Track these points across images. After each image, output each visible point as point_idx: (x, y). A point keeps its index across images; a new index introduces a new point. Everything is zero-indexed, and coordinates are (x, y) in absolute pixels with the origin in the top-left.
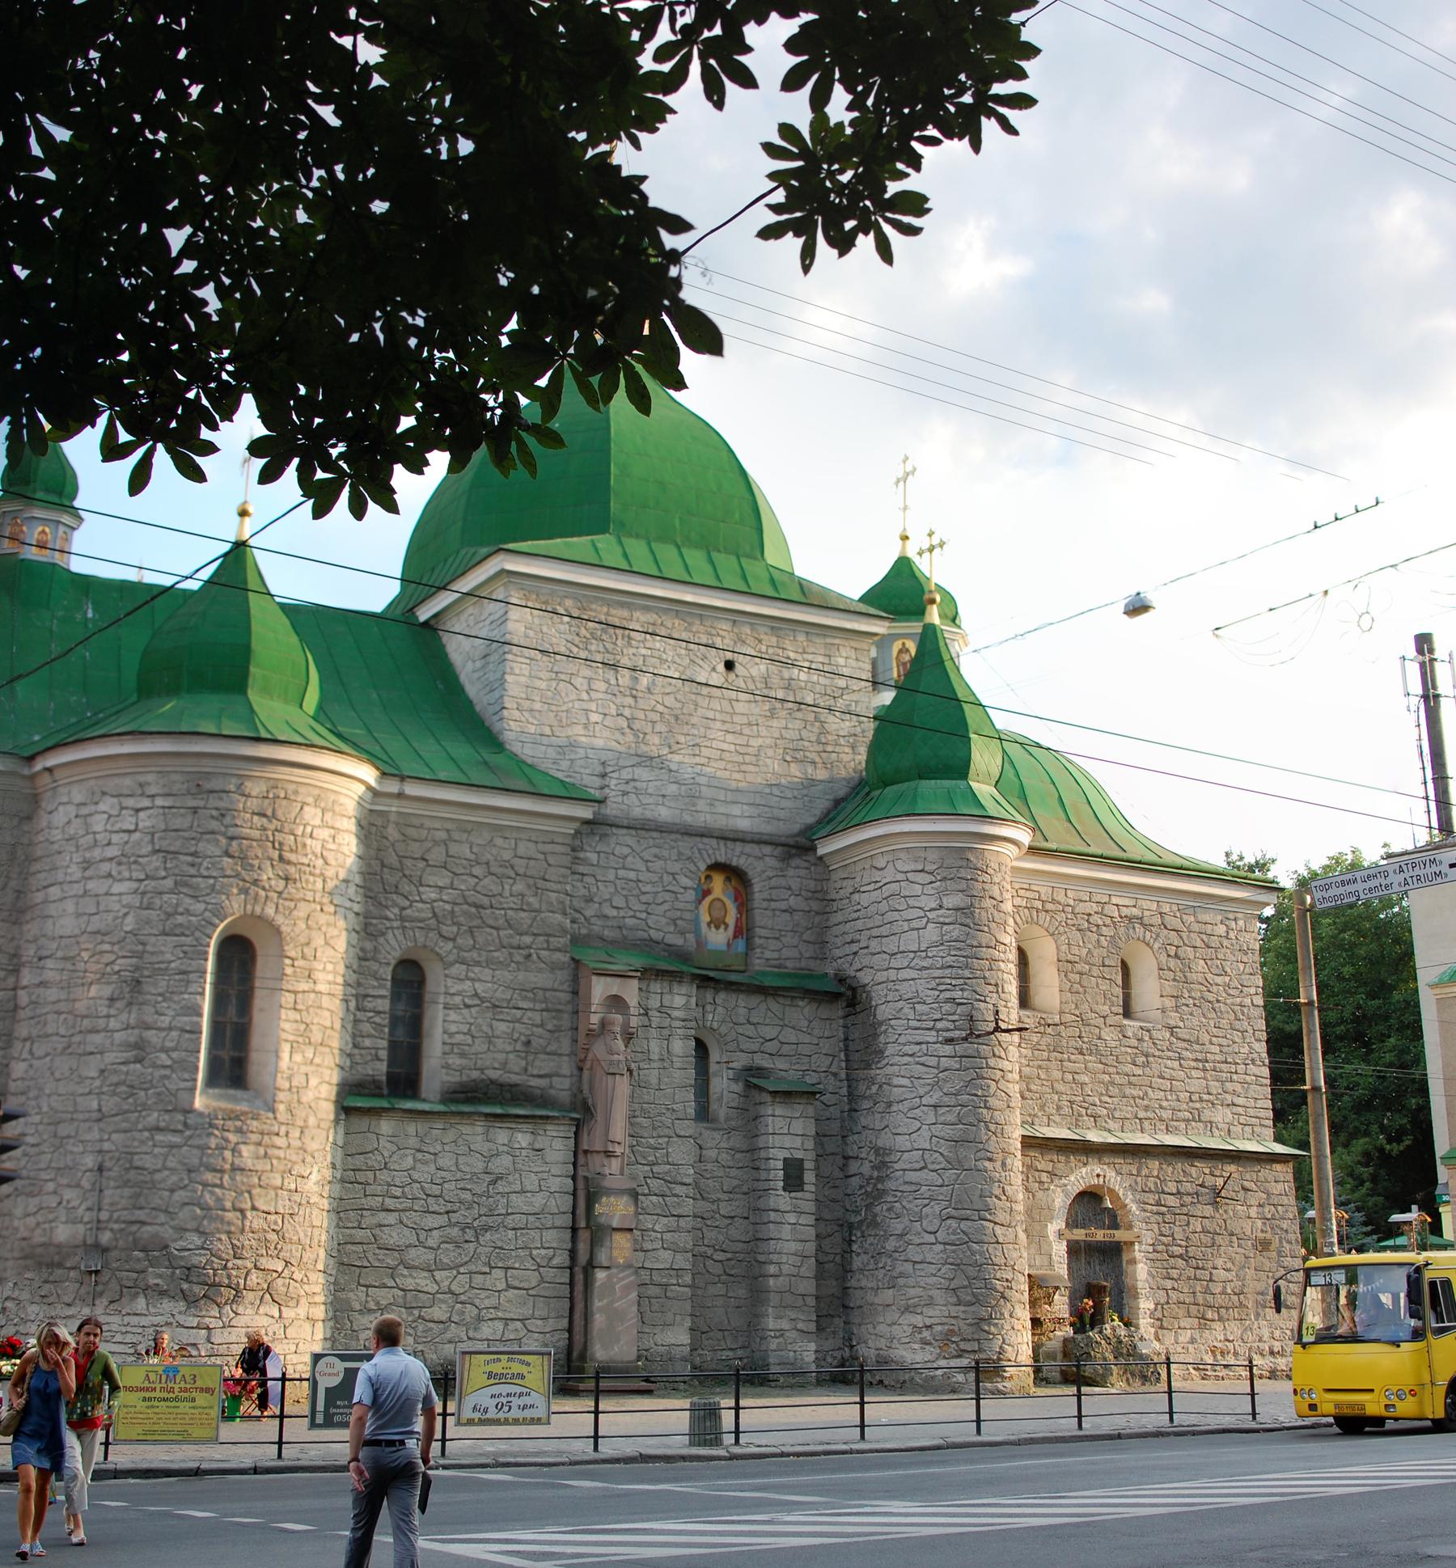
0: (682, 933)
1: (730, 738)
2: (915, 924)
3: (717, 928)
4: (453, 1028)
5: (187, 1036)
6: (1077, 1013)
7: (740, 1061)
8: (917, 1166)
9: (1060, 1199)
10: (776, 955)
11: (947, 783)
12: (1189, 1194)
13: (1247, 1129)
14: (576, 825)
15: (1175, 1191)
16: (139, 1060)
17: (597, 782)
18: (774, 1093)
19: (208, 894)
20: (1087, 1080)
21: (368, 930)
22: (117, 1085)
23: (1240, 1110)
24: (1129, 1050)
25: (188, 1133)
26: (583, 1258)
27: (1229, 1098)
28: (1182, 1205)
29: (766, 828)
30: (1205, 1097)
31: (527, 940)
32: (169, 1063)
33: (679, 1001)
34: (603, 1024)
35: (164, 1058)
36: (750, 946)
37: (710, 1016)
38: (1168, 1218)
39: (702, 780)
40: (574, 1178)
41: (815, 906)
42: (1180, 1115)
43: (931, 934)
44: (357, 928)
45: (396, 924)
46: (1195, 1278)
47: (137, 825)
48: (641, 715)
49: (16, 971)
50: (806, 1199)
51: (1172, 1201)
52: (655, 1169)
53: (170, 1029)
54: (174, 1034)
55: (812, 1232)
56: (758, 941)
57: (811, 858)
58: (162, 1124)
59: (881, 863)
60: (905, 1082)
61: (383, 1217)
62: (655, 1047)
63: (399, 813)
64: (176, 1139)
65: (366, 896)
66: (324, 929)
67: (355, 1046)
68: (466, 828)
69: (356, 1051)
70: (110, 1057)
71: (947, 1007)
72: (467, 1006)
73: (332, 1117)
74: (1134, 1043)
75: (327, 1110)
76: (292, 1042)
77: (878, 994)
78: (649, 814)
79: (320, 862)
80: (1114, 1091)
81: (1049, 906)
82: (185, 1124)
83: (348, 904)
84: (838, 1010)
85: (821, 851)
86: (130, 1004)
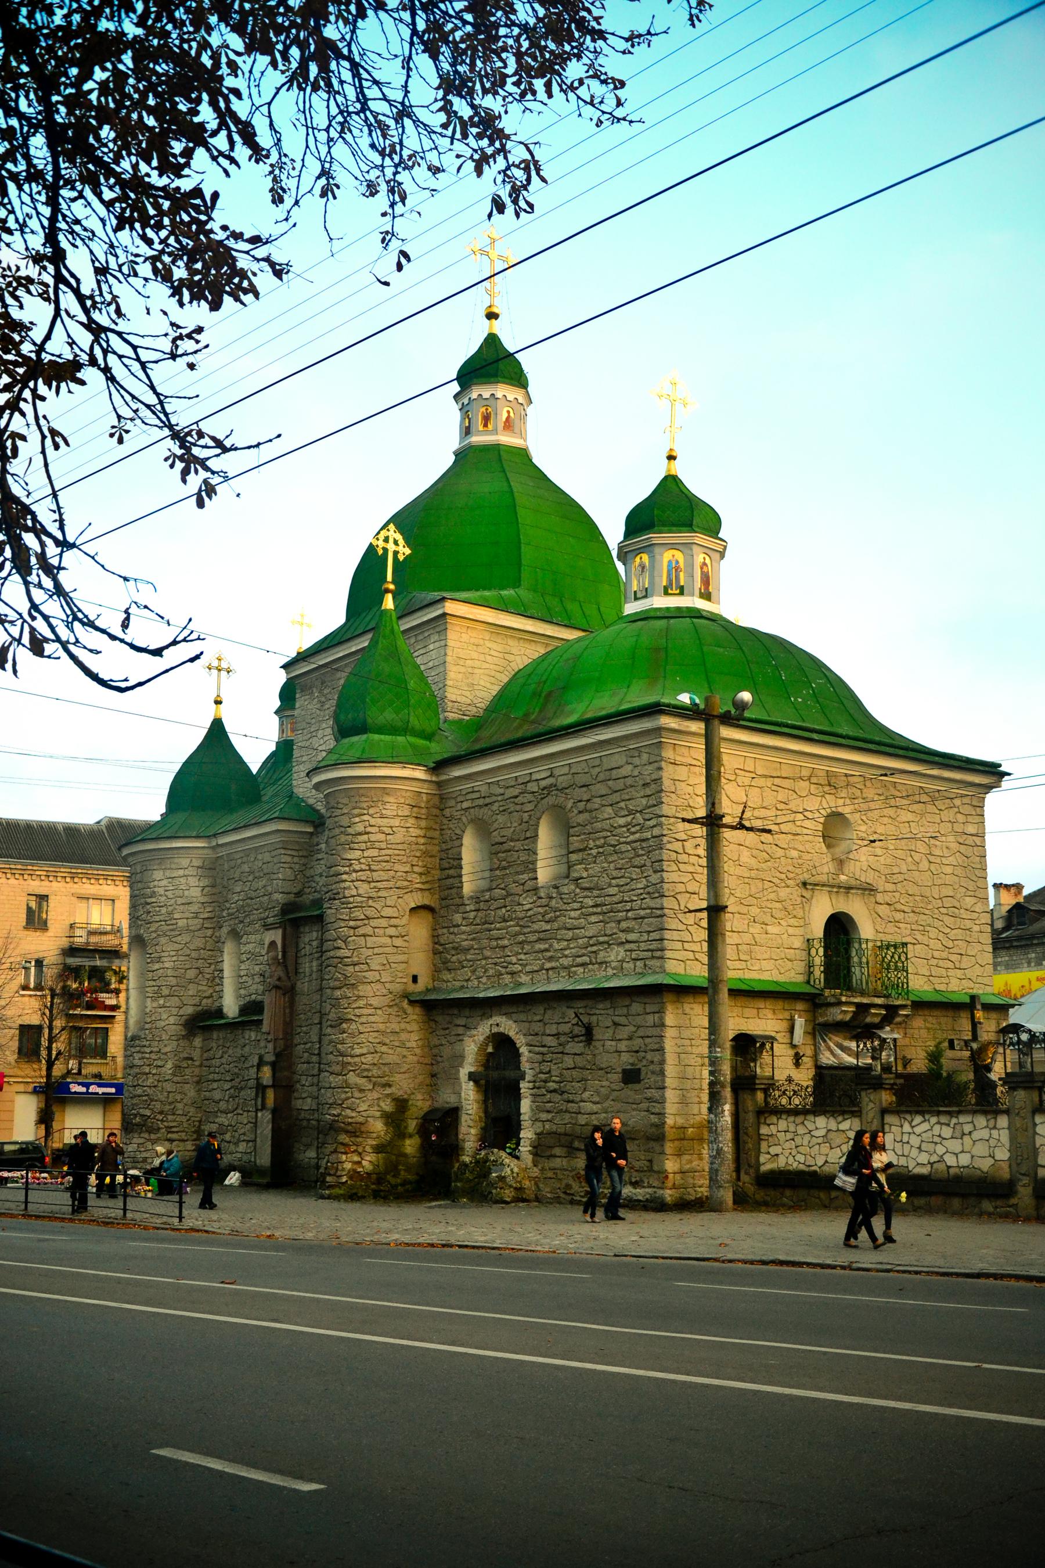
6: (502, 886)
12: (565, 1034)
13: (638, 963)
15: (554, 1032)
20: (506, 942)
23: (633, 946)
24: (541, 910)
27: (623, 937)
28: (560, 1045)
30: (601, 939)
38: (548, 1057)
42: (579, 960)
46: (566, 1111)
51: (550, 1041)
68: (247, 853)
74: (544, 901)
75: (174, 1030)
80: (527, 947)
81: (488, 800)
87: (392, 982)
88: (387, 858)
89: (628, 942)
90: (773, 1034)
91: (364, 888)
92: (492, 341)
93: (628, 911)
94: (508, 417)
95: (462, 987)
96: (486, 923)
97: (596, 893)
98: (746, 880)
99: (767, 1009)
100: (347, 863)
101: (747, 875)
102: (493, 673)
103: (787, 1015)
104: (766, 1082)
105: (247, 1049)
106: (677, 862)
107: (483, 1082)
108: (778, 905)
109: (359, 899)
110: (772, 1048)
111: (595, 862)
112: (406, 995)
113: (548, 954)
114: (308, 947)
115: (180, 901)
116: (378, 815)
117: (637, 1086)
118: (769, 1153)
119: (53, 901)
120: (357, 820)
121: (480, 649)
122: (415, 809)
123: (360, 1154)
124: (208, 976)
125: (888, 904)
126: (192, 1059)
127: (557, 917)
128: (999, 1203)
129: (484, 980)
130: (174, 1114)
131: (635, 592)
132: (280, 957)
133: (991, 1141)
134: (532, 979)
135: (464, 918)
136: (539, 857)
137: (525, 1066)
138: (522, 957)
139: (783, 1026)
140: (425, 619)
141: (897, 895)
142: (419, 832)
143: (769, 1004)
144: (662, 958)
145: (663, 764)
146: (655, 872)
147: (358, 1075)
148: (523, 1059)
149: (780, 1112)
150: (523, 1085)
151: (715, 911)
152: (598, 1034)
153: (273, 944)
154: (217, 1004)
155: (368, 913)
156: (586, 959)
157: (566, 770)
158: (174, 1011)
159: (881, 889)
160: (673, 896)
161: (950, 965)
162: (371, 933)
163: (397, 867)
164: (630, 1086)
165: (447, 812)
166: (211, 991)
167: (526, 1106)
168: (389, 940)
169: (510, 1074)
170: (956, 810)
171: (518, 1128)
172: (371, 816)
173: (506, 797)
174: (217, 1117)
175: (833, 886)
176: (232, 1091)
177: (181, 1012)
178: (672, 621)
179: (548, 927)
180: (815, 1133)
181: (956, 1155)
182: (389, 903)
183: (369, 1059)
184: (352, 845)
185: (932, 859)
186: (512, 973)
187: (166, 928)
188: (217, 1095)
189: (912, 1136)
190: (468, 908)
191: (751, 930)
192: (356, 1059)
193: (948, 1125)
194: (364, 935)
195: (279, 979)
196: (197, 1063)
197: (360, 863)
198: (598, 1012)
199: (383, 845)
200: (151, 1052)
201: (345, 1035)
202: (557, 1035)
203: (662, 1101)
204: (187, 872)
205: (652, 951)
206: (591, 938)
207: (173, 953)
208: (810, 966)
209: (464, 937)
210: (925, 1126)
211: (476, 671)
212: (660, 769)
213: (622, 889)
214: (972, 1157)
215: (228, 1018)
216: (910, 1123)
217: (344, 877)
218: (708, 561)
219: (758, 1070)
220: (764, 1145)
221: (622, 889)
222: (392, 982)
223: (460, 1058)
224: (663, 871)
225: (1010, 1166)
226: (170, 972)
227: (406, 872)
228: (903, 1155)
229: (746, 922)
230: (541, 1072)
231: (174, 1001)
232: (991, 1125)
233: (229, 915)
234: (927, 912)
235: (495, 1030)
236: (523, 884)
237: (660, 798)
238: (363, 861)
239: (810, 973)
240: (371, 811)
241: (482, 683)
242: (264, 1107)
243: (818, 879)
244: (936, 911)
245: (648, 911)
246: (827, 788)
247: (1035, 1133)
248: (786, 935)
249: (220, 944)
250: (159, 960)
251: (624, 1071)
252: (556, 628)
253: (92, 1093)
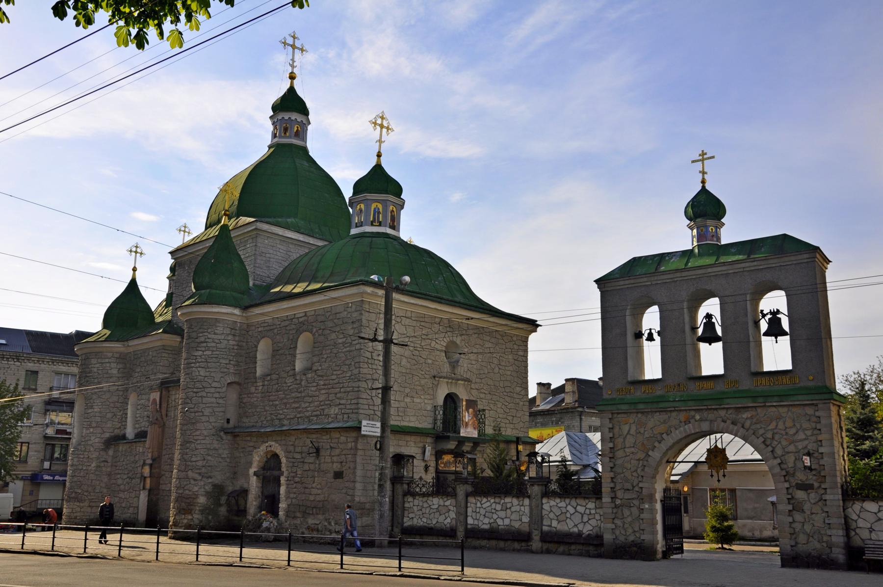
4: (137, 415)
6: (277, 373)
9: (257, 459)
13: (346, 416)
23: (342, 407)
24: (296, 386)
27: (338, 401)
28: (302, 458)
30: (327, 402)
42: (315, 413)
46: (304, 493)
51: (298, 456)
52: (170, 456)
63: (133, 351)
68: (145, 351)
79: (96, 374)
81: (272, 327)
87: (215, 422)
88: (217, 356)
89: (340, 404)
90: (414, 455)
91: (203, 372)
92: (291, 91)
93: (341, 388)
94: (297, 130)
95: (253, 426)
96: (267, 392)
97: (325, 378)
98: (404, 374)
99: (411, 439)
100: (195, 358)
101: (404, 371)
102: (280, 261)
103: (421, 445)
104: (409, 479)
105: (137, 457)
106: (368, 363)
107: (261, 477)
108: (420, 388)
109: (200, 377)
110: (413, 462)
111: (325, 362)
112: (223, 429)
113: (299, 410)
114: (173, 402)
115: (105, 376)
116: (213, 333)
117: (341, 480)
118: (408, 517)
119: (40, 375)
120: (201, 335)
121: (274, 249)
122: (233, 331)
123: (192, 515)
124: (118, 417)
125: (477, 389)
126: (107, 462)
127: (304, 390)
128: (523, 544)
129: (265, 422)
130: (94, 492)
131: (356, 223)
132: (158, 407)
133: (521, 512)
134: (290, 423)
135: (256, 389)
136: (297, 358)
137: (284, 469)
138: (286, 411)
139: (420, 451)
140: (246, 231)
141: (482, 385)
142: (234, 343)
143: (413, 438)
144: (357, 413)
145: (363, 312)
146: (356, 368)
147: (193, 472)
148: (283, 465)
149: (414, 495)
150: (283, 480)
151: (386, 389)
152: (322, 453)
153: (154, 400)
154: (122, 432)
155: (204, 385)
156: (318, 413)
157: (313, 313)
158: (99, 435)
159: (474, 381)
160: (365, 381)
161: (508, 422)
162: (205, 395)
163: (221, 361)
164: (337, 480)
165: (250, 333)
166: (120, 425)
167: (283, 489)
168: (214, 400)
169: (276, 473)
170: (514, 343)
171: (279, 502)
172: (209, 333)
173: (281, 326)
174: (118, 493)
175: (449, 378)
176: (128, 479)
177: (103, 436)
178: (374, 239)
179: (300, 395)
180: (433, 507)
181: (503, 519)
182: (216, 380)
183: (200, 463)
184: (198, 348)
185: (500, 367)
186: (280, 420)
188: (120, 482)
189: (482, 509)
190: (258, 384)
191: (406, 400)
192: (194, 463)
193: (499, 503)
194: (201, 397)
195: (157, 419)
196: (109, 464)
197: (201, 358)
198: (323, 441)
199: (215, 349)
201: (188, 450)
202: (301, 453)
203: (354, 489)
204: (110, 361)
205: (353, 409)
206: (321, 401)
207: (100, 404)
208: (435, 420)
209: (255, 399)
210: (488, 504)
211: (271, 260)
212: (361, 314)
213: (338, 376)
214: (511, 520)
215: (128, 439)
216: (480, 502)
217: (193, 365)
218: (394, 209)
219: (405, 474)
220: (406, 513)
221: (338, 376)
222: (215, 422)
223: (250, 464)
224: (360, 368)
225: (529, 526)
226: (97, 414)
227: (226, 364)
228: (476, 519)
229: (403, 396)
230: (292, 472)
231: (99, 430)
232: (521, 504)
234: (497, 394)
235: (269, 449)
236: (288, 372)
237: (361, 329)
238: (203, 357)
239: (435, 423)
240: (209, 331)
241: (274, 266)
242: (144, 488)
243: (441, 374)
244: (501, 394)
245: (351, 388)
246: (448, 329)
247: (542, 508)
248: (423, 404)
249: (126, 400)
250: (92, 407)
251: (335, 472)
252: (316, 240)
253: (56, 480)
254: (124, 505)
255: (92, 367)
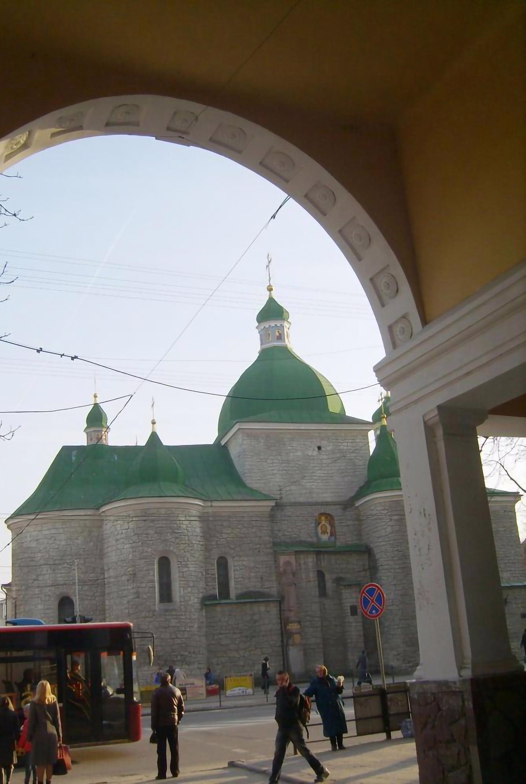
0: (312, 537)
1: (322, 472)
2: (384, 527)
3: (324, 534)
4: (237, 577)
5: (151, 589)
7: (334, 576)
8: (391, 604)
10: (344, 540)
11: (390, 479)
14: (270, 508)
16: (138, 597)
17: (279, 492)
18: (345, 586)
19: (152, 546)
21: (207, 549)
22: (132, 605)
25: (154, 617)
26: (285, 643)
29: (336, 499)
31: (258, 546)
32: (146, 597)
33: (310, 560)
34: (285, 570)
35: (145, 597)
36: (335, 538)
37: (323, 564)
39: (313, 487)
40: (280, 619)
41: (356, 522)
43: (389, 529)
44: (202, 549)
45: (215, 546)
47: (129, 527)
48: (290, 468)
49: (104, 574)
50: (359, 618)
53: (145, 587)
54: (147, 589)
55: (361, 628)
56: (337, 537)
57: (354, 508)
58: (147, 615)
59: (372, 508)
60: (385, 578)
61: (221, 636)
62: (304, 576)
63: (212, 512)
64: (152, 619)
65: (205, 539)
66: (190, 551)
67: (207, 585)
69: (207, 587)
70: (131, 597)
71: (396, 553)
72: (241, 569)
73: (200, 608)
75: (198, 606)
76: (183, 587)
77: (376, 551)
78: (297, 500)
82: (154, 615)
83: (198, 543)
84: (366, 556)
85: (356, 505)
86: (134, 581)
114: (303, 566)
130: (199, 654)
187: (190, 548)
200: (186, 618)
226: (193, 574)
233: (217, 544)
250: (186, 566)
254: (241, 663)
255: (180, 524)
